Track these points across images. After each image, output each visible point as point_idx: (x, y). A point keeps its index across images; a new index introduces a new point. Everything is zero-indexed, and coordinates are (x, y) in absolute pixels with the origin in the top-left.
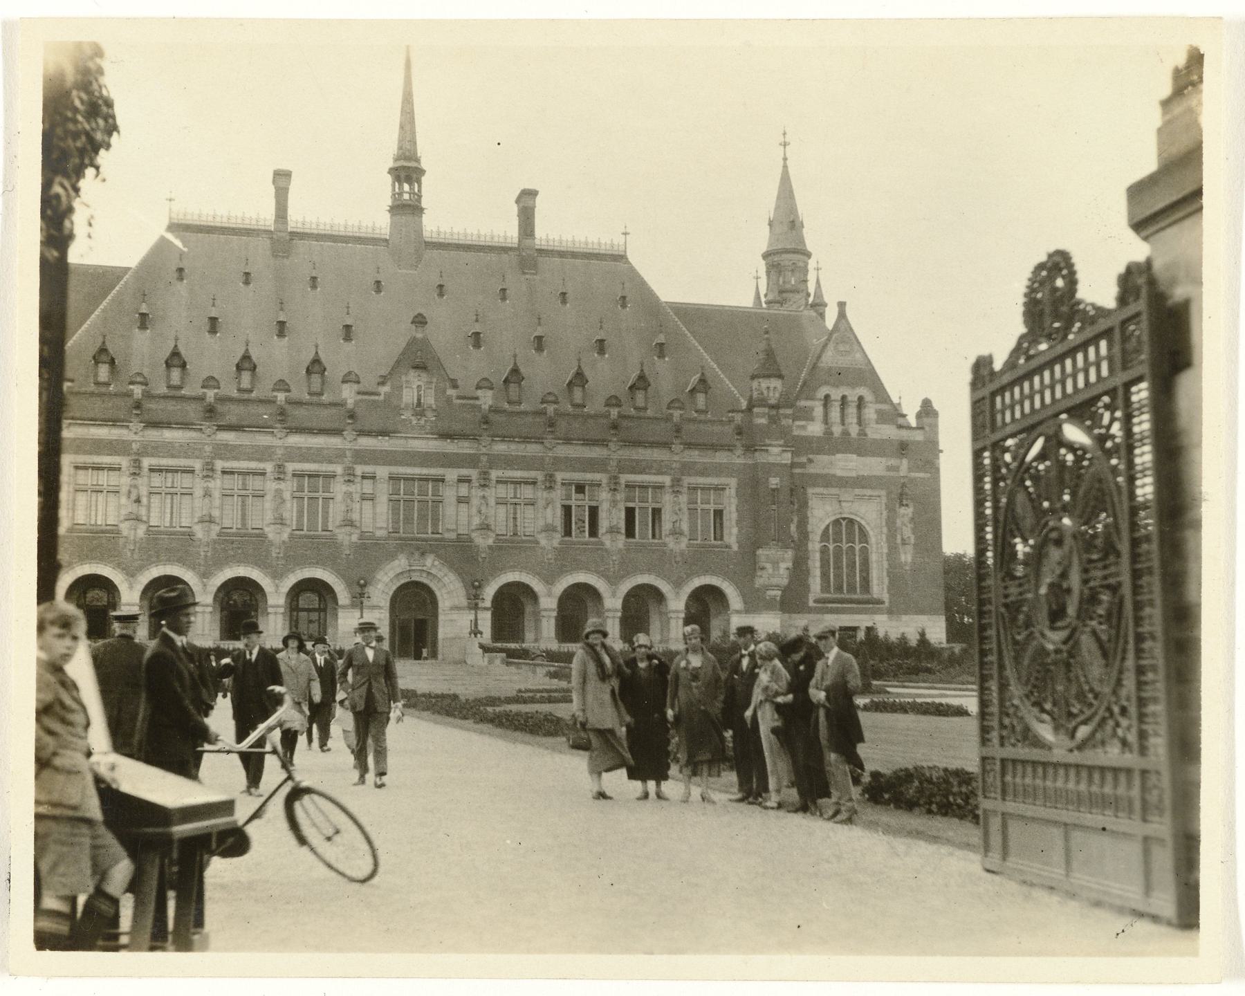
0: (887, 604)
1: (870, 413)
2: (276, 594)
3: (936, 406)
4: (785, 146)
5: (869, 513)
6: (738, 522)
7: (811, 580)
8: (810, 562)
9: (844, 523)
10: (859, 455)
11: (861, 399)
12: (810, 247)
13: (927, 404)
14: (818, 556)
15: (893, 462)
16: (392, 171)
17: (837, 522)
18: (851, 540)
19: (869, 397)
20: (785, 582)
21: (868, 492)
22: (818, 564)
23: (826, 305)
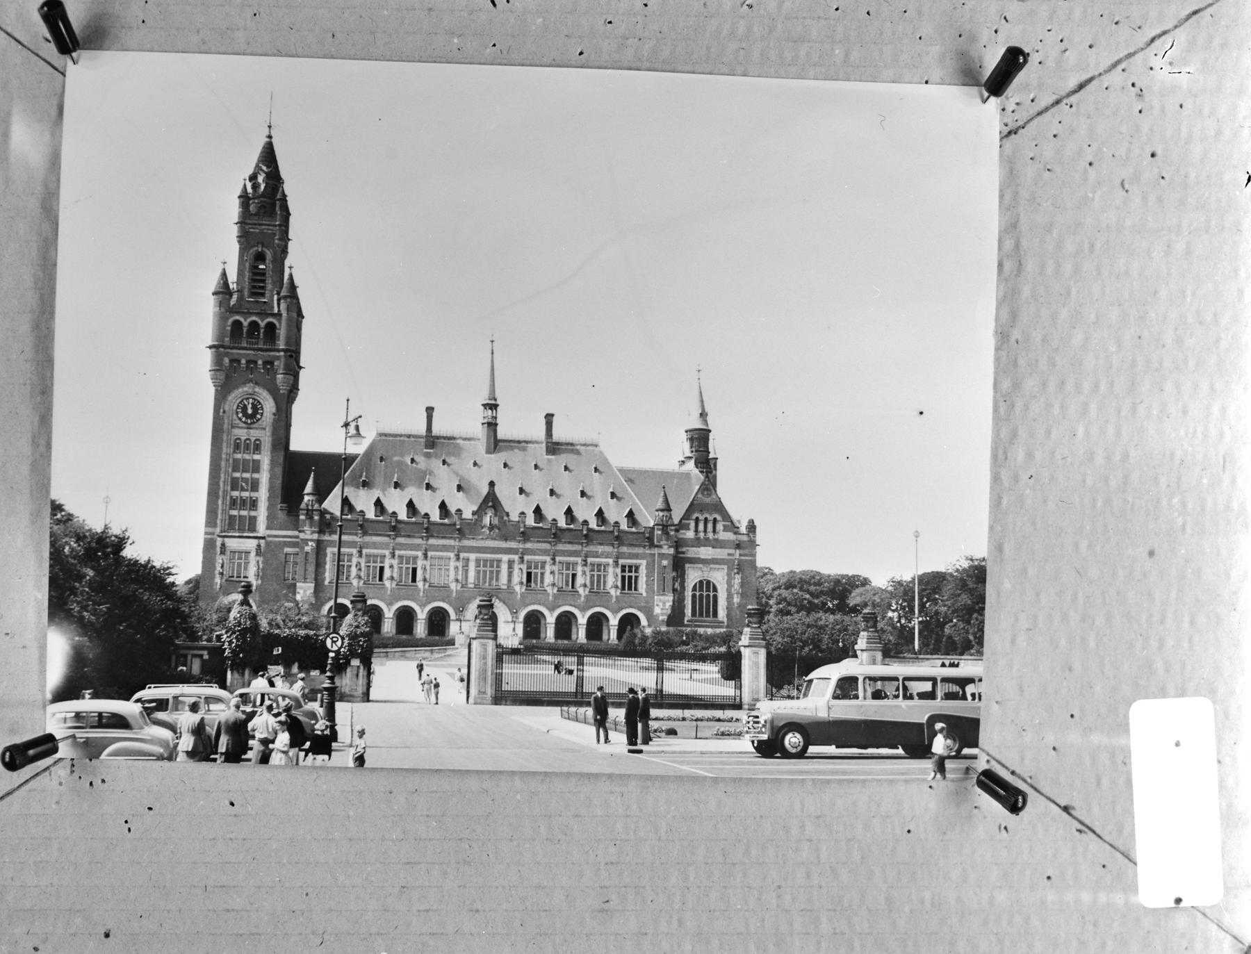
0: (726, 624)
1: (720, 526)
2: (422, 615)
3: (756, 524)
5: (719, 577)
7: (686, 611)
8: (686, 602)
10: (713, 547)
11: (715, 520)
14: (690, 598)
15: (732, 551)
16: (483, 405)
17: (701, 582)
18: (708, 590)
19: (719, 518)
20: (669, 612)
21: (717, 566)
22: (690, 602)
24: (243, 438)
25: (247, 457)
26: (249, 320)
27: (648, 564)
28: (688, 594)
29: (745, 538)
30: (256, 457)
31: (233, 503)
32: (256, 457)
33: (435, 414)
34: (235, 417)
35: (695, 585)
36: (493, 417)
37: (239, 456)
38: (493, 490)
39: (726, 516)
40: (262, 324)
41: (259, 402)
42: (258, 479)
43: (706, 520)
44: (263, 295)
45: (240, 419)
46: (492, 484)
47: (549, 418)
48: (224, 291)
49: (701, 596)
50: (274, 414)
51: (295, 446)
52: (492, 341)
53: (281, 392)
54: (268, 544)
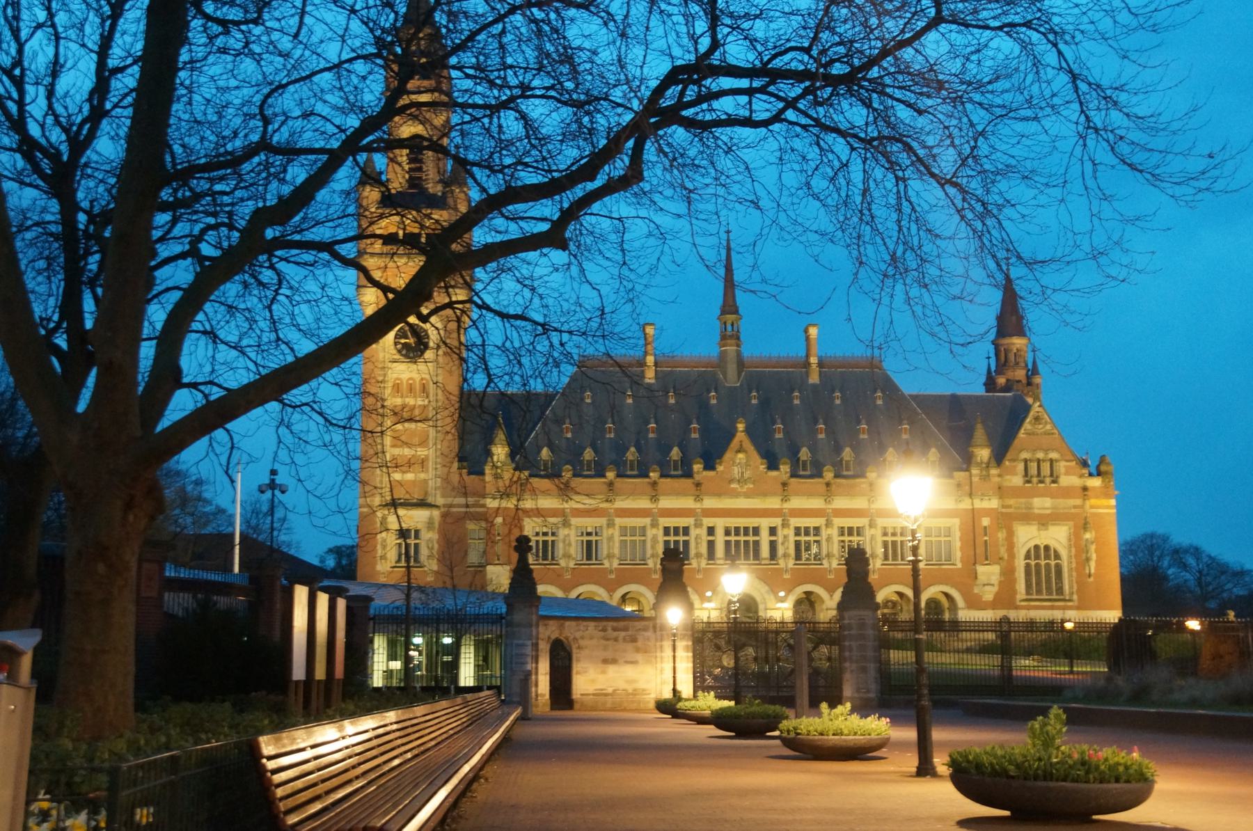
1: (1061, 466)
6: (962, 549)
7: (1017, 587)
8: (1017, 574)
9: (1042, 546)
15: (1078, 502)
17: (1037, 547)
18: (1047, 557)
19: (1054, 455)
27: (962, 524)
28: (1020, 563)
35: (1029, 552)
43: (1039, 461)
49: (1037, 565)
54: (444, 516)
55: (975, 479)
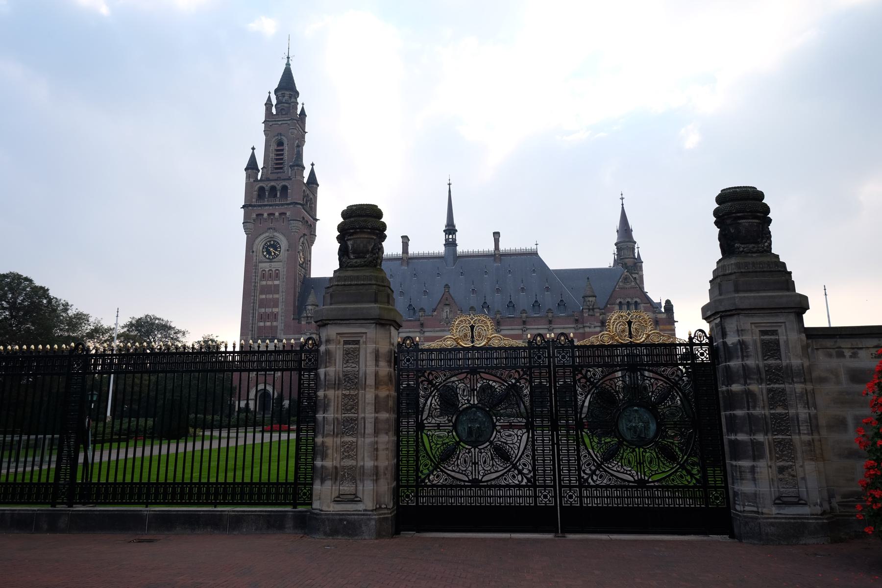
4: (622, 199)
12: (635, 238)
13: (668, 302)
16: (444, 231)
19: (638, 300)
23: (642, 262)
24: (267, 270)
25: (270, 283)
26: (269, 186)
29: (664, 316)
30: (276, 282)
31: (262, 318)
32: (276, 282)
33: (410, 243)
34: (261, 253)
36: (452, 238)
37: (264, 283)
38: (448, 291)
39: (648, 300)
40: (279, 187)
41: (277, 243)
42: (278, 299)
43: (628, 302)
44: (281, 168)
45: (265, 256)
46: (447, 286)
47: (497, 235)
48: (252, 166)
50: (288, 250)
51: (311, 277)
52: (449, 184)
53: (292, 234)
55: (586, 315)
